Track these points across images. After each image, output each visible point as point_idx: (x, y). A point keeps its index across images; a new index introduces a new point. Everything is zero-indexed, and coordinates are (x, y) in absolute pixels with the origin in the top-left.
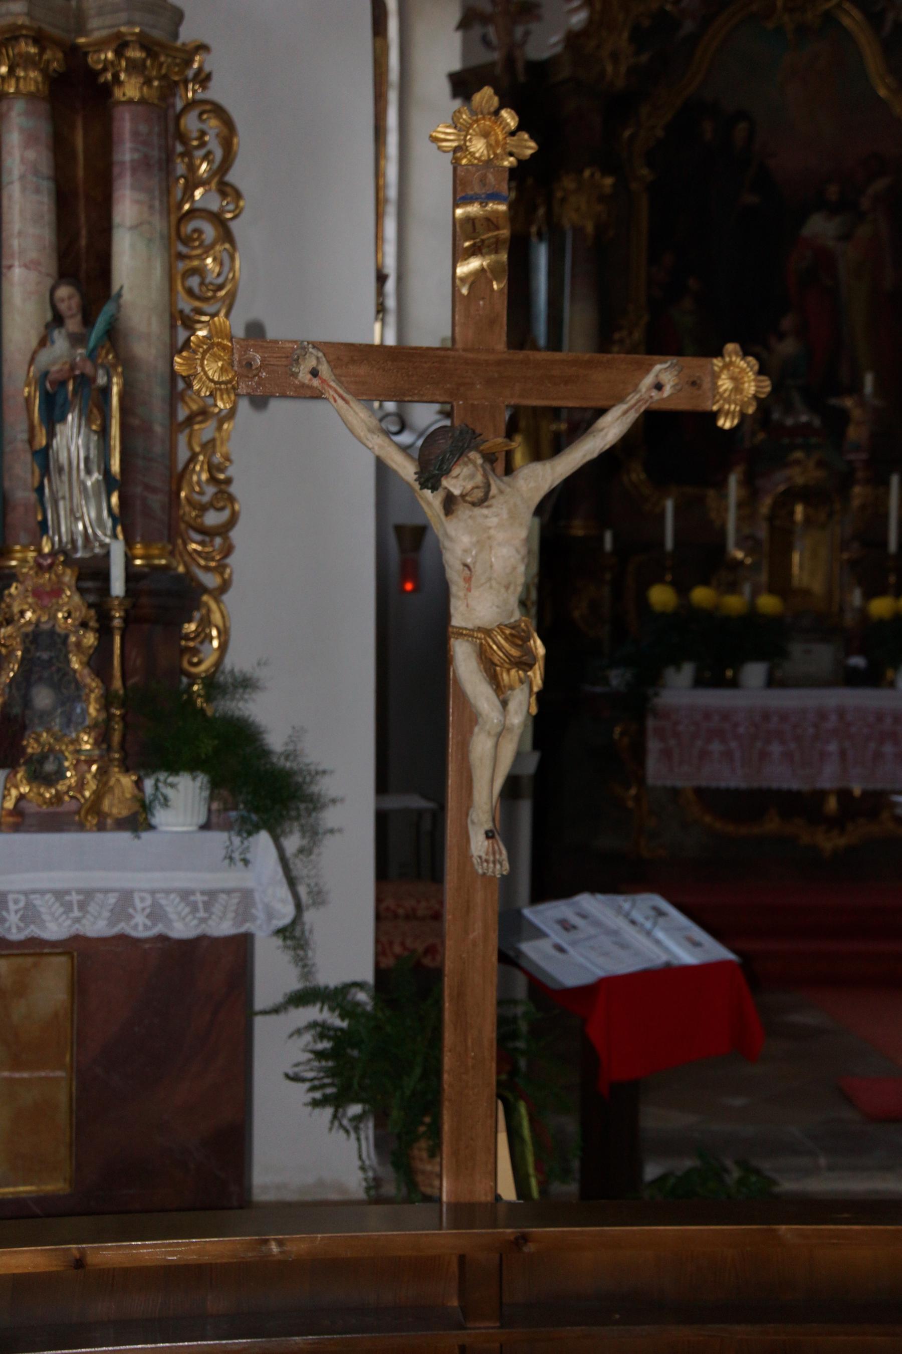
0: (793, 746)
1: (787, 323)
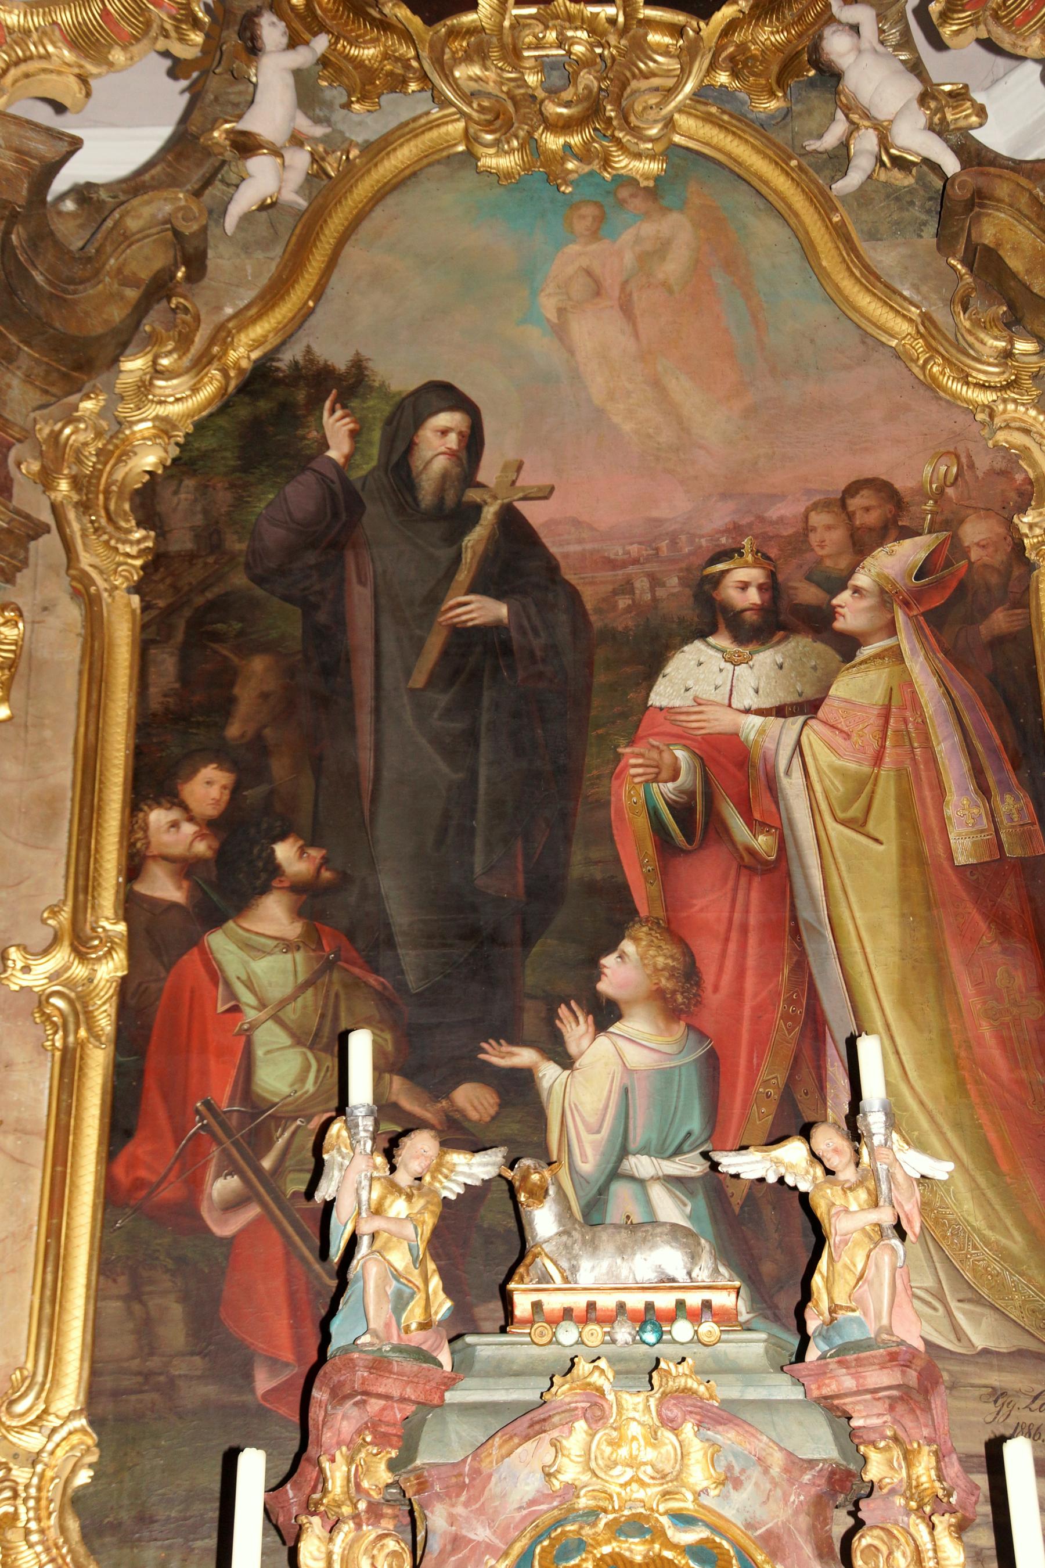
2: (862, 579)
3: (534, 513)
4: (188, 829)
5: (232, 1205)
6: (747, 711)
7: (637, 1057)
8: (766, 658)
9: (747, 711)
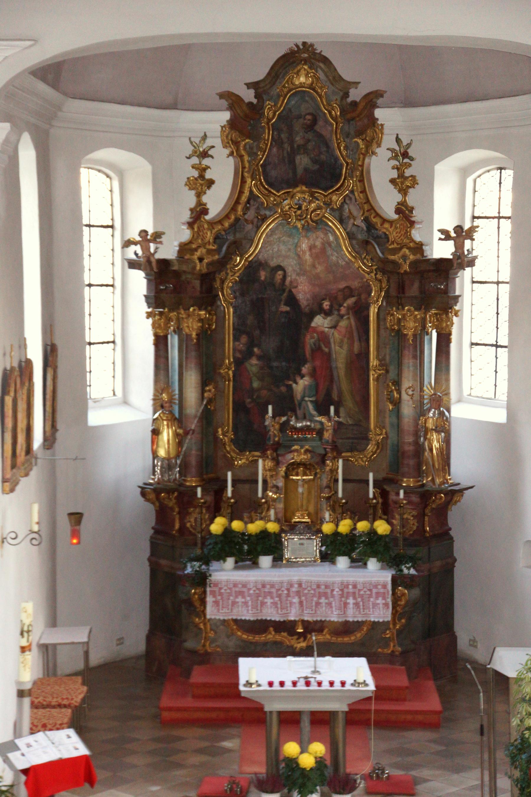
0: (277, 599)
1: (305, 370)
2: (345, 305)
3: (293, 290)
4: (241, 345)
5: (250, 403)
6: (326, 328)
7: (306, 383)
8: (329, 318)
9: (326, 328)
